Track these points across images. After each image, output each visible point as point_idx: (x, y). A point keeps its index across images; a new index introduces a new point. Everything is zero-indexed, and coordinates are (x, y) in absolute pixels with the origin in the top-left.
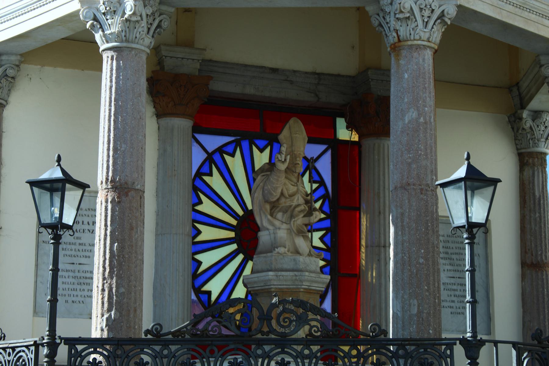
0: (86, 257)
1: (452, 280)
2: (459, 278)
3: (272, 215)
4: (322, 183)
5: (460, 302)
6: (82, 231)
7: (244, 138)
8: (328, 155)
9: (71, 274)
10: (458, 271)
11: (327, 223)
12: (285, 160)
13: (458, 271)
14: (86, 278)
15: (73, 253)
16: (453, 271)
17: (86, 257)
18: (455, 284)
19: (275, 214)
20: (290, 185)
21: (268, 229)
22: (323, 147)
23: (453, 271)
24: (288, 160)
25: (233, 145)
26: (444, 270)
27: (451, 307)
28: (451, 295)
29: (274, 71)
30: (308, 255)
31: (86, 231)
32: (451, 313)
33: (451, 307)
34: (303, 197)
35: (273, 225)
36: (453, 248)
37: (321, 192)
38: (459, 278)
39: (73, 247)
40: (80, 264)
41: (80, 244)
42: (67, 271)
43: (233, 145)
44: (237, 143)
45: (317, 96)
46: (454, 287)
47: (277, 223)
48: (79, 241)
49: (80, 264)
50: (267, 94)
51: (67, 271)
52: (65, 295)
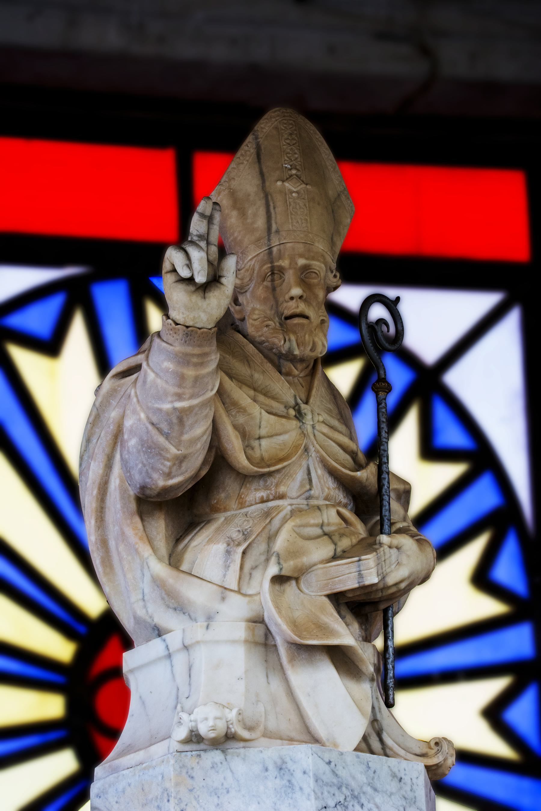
3: (174, 560)
4: (481, 458)
7: (104, 273)
8: (508, 336)
11: (517, 642)
12: (215, 280)
19: (188, 557)
20: (256, 410)
21: (159, 632)
22: (482, 302)
24: (229, 281)
25: (52, 306)
30: (365, 745)
34: (332, 473)
35: (179, 606)
37: (482, 497)
43: (52, 306)
44: (76, 296)
45: (425, 51)
47: (196, 593)
50: (185, 50)
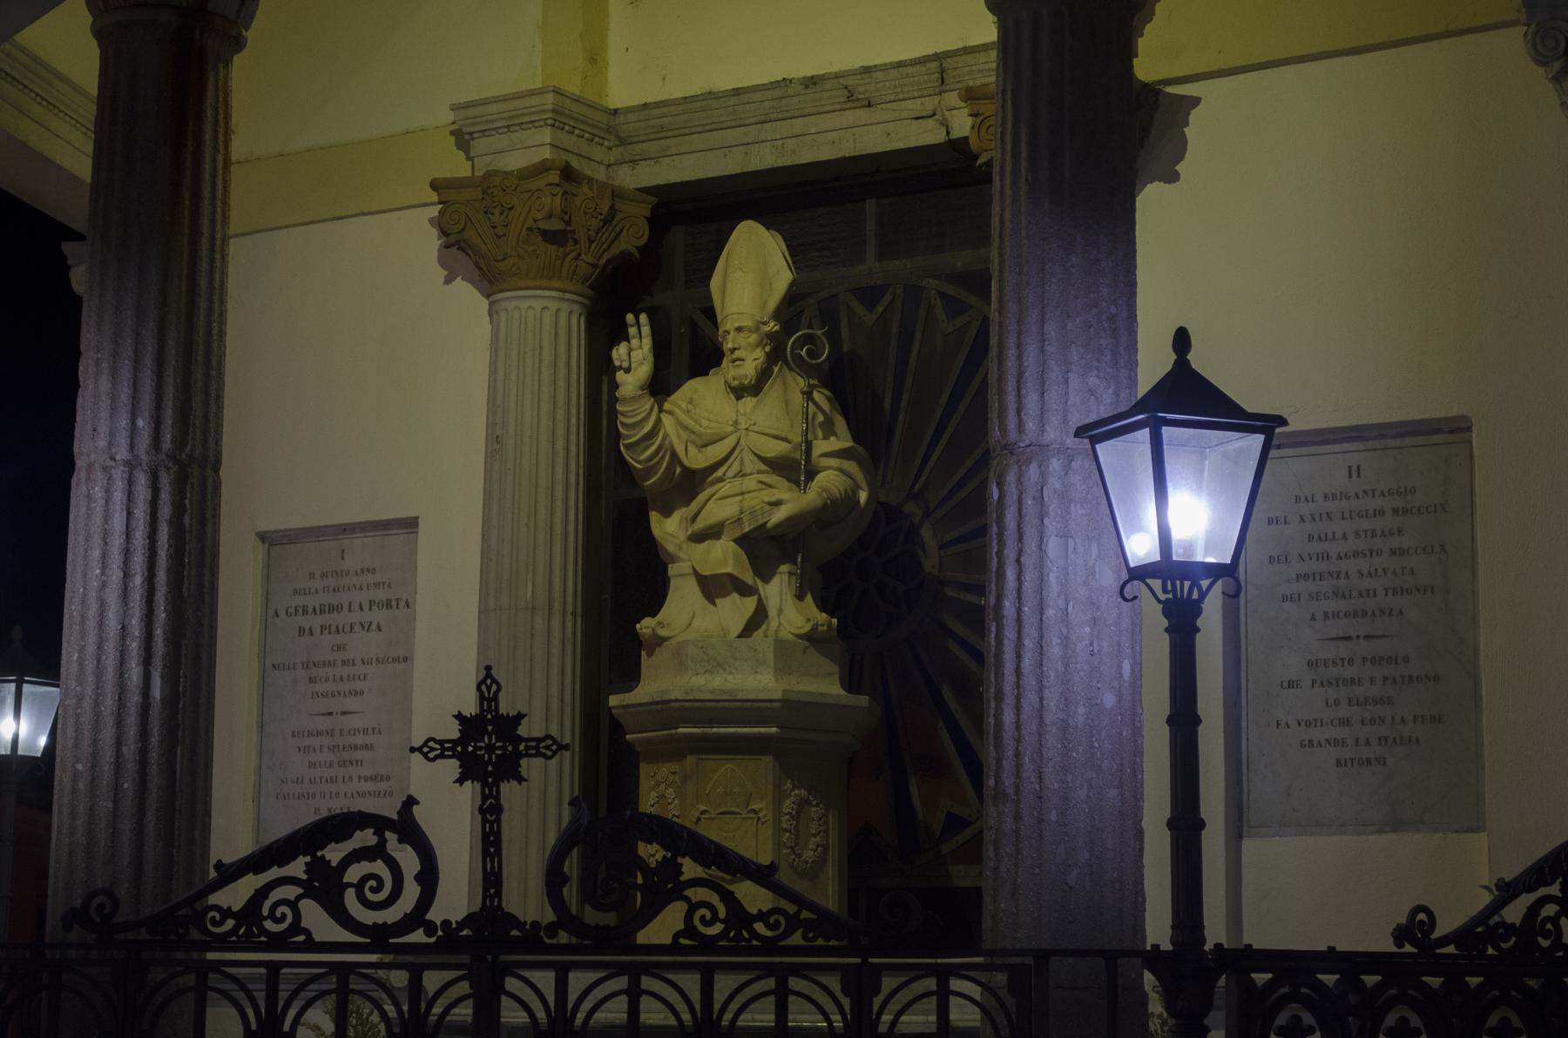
0: (356, 693)
1: (1344, 649)
2: (1366, 637)
5: (1372, 722)
6: (347, 628)
9: (326, 741)
10: (1365, 613)
13: (1365, 613)
14: (356, 747)
15: (329, 687)
16: (1347, 615)
17: (356, 693)
18: (1351, 662)
23: (1347, 615)
26: (1313, 618)
27: (1337, 743)
28: (1337, 702)
29: (812, 82)
31: (357, 628)
32: (1338, 763)
33: (1337, 743)
36: (1345, 537)
38: (1366, 637)
39: (330, 671)
40: (344, 713)
41: (344, 662)
42: (319, 734)
46: (1349, 672)
48: (342, 655)
49: (344, 713)
51: (319, 734)
52: (314, 796)
